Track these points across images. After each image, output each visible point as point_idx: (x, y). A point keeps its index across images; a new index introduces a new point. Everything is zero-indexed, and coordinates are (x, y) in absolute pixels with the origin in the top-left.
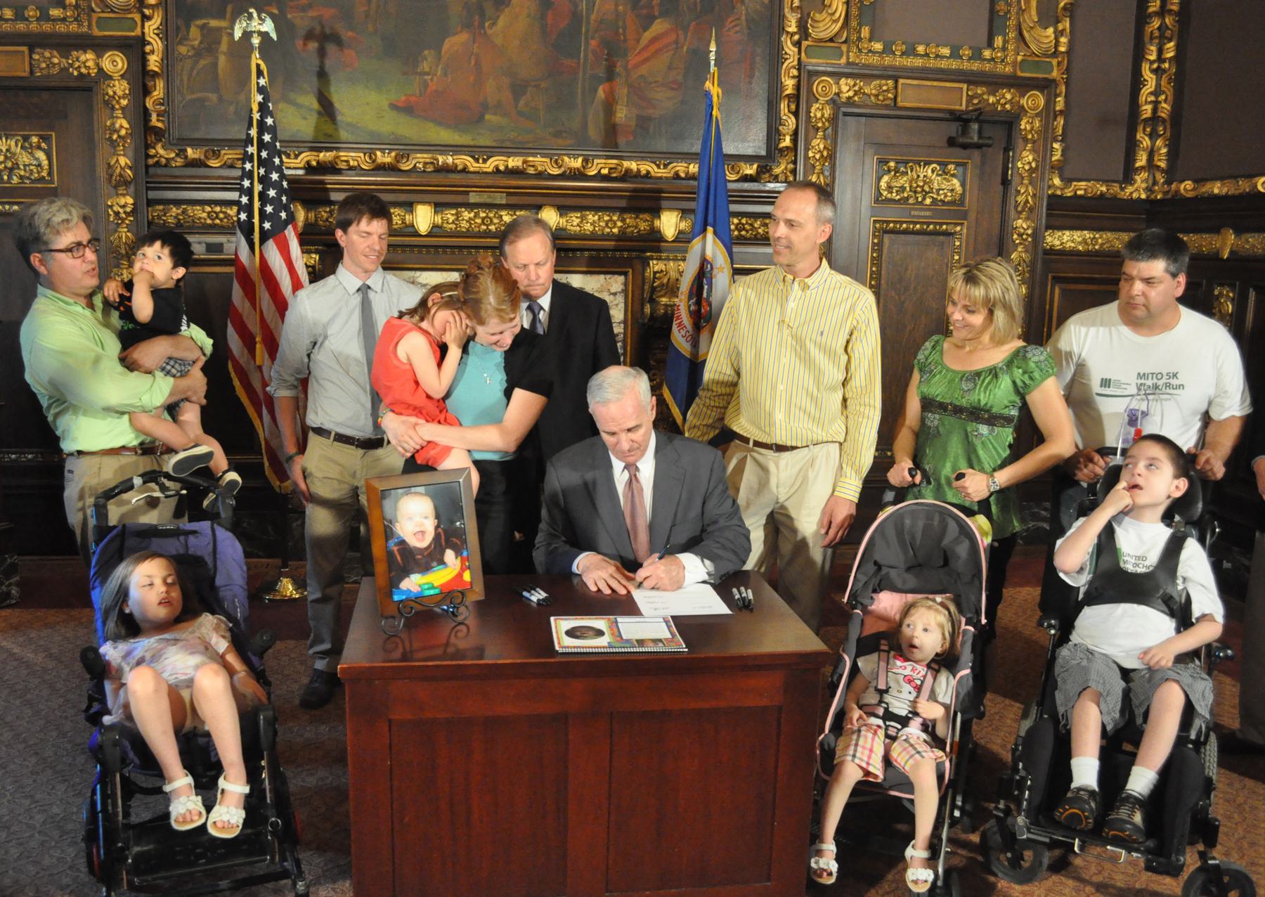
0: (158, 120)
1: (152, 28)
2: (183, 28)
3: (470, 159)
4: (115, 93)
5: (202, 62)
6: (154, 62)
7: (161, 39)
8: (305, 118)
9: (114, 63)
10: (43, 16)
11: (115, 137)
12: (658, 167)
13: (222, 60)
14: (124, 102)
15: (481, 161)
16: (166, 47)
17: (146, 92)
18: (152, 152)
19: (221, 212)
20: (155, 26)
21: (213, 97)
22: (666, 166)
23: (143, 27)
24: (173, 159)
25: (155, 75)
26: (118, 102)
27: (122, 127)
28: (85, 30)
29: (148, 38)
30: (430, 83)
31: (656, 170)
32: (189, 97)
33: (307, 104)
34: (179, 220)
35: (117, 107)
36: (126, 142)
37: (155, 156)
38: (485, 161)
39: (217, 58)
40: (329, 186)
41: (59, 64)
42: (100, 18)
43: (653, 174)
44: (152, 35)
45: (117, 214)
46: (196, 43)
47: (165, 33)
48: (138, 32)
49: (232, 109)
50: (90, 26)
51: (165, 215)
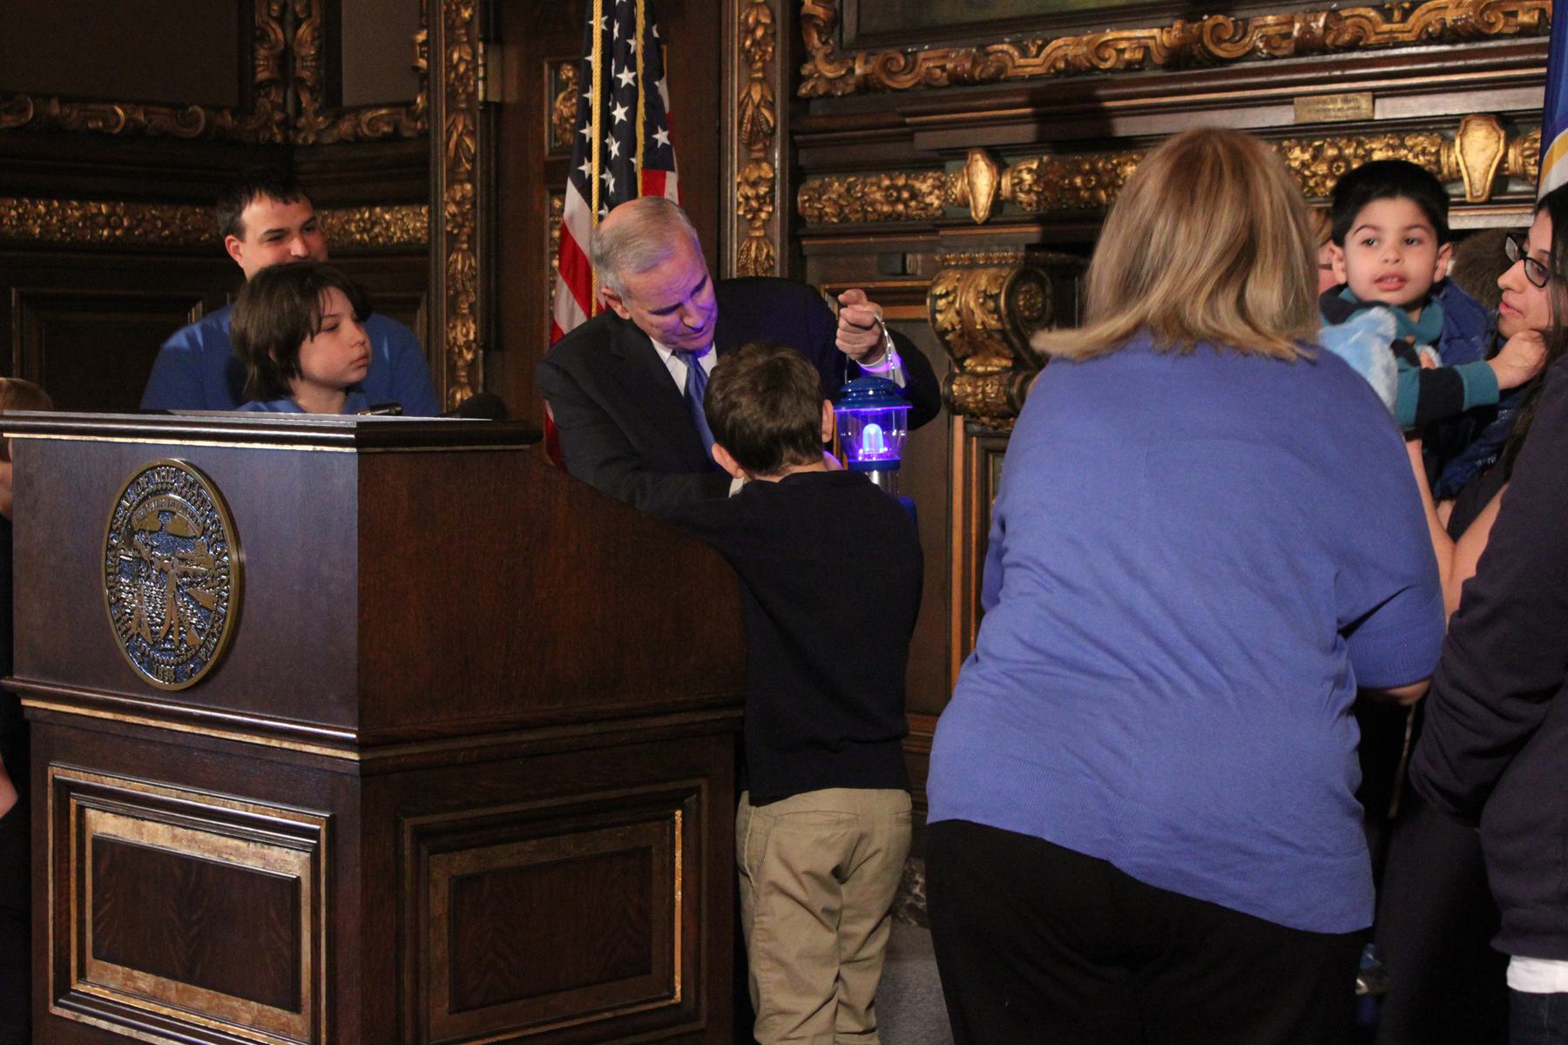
3: (1372, 14)
11: (748, 43)
15: (1397, 15)
18: (806, 70)
19: (905, 186)
24: (842, 77)
27: (758, 22)
34: (841, 207)
36: (765, 52)
37: (810, 76)
38: (1406, 15)
45: (747, 198)
51: (819, 199)
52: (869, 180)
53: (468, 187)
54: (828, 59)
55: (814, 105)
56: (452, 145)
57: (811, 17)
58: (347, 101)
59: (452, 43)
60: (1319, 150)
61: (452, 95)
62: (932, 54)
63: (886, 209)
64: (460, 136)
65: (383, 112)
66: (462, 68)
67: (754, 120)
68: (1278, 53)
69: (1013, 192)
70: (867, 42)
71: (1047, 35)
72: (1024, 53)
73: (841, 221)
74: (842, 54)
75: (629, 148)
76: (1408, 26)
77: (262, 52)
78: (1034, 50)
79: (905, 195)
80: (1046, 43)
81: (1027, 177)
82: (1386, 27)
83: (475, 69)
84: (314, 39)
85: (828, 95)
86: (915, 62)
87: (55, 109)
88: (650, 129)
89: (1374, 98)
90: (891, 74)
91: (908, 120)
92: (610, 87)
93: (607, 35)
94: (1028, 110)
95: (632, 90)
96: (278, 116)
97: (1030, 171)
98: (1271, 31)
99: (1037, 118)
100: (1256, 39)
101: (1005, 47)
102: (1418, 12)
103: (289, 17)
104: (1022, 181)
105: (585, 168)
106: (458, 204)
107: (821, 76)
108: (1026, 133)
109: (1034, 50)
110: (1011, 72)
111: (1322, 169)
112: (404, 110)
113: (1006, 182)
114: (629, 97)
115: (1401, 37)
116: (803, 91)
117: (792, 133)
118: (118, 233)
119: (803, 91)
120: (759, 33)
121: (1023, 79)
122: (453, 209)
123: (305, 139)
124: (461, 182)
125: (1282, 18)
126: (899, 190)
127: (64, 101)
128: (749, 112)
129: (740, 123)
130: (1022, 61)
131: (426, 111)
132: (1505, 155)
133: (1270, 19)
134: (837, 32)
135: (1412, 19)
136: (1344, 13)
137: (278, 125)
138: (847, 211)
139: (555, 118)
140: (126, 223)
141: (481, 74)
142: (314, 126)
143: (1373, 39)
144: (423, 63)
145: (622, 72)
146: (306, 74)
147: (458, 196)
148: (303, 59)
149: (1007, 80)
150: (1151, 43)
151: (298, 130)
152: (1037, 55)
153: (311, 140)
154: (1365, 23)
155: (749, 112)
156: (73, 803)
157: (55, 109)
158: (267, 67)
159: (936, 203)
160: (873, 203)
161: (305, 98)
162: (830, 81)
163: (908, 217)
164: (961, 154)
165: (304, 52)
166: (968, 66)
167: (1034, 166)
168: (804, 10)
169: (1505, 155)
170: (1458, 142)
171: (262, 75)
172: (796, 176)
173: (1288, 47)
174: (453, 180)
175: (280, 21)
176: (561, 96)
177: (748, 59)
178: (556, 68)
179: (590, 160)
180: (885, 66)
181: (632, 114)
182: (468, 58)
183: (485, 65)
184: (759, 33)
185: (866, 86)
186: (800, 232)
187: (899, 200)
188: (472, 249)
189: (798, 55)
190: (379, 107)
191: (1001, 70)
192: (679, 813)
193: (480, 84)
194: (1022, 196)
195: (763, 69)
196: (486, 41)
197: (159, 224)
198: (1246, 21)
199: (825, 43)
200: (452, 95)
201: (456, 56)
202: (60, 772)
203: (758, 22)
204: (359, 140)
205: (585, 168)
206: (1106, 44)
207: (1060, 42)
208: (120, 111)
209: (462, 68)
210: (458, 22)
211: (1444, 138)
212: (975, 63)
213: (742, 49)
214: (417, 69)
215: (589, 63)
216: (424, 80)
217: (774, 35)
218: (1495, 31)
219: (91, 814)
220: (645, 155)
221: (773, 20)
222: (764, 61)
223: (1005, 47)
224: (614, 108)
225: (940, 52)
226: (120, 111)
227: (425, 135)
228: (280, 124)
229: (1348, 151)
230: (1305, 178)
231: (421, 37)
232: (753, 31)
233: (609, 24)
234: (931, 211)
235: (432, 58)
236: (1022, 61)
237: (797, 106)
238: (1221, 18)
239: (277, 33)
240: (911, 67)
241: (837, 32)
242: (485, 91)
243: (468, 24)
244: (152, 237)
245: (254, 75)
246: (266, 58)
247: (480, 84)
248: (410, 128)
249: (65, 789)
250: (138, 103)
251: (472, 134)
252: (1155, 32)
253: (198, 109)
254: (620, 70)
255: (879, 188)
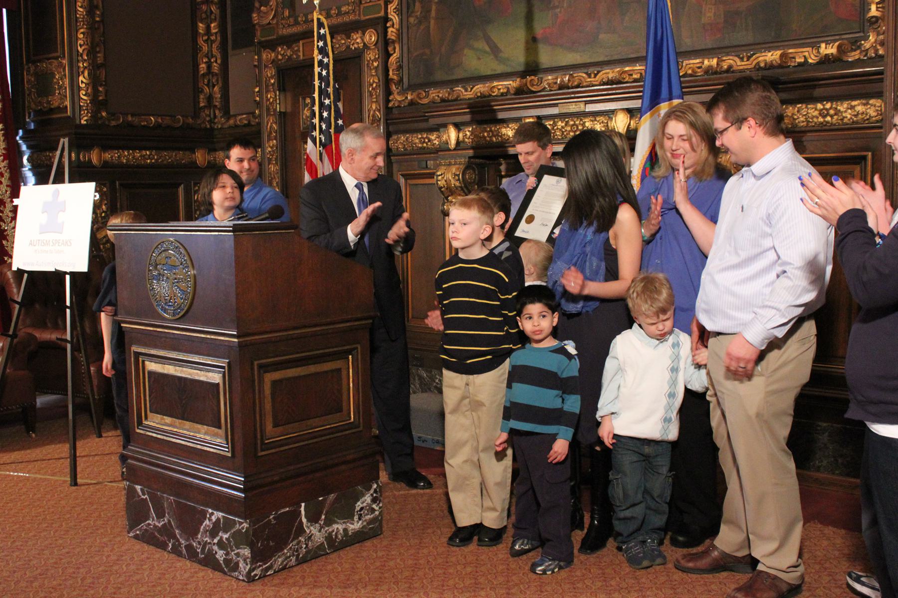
0: (393, 74)
1: (393, 8)
2: (412, 5)
3: (584, 75)
4: (370, 58)
5: (422, 27)
6: (392, 33)
7: (398, 15)
8: (479, 59)
9: (371, 37)
10: (339, 14)
11: (370, 89)
12: (742, 59)
13: (432, 22)
14: (375, 64)
15: (593, 76)
16: (401, 21)
17: (388, 55)
19: (427, 137)
20: (394, 7)
21: (427, 51)
22: (749, 58)
23: (386, 9)
24: (404, 100)
25: (393, 42)
26: (372, 64)
27: (374, 82)
28: (357, 17)
29: (390, 16)
30: (559, 15)
31: (739, 63)
32: (415, 54)
33: (480, 47)
34: (404, 145)
35: (372, 68)
36: (376, 92)
37: (392, 100)
38: (596, 75)
39: (430, 22)
40: (495, 108)
41: (345, 43)
42: (364, 7)
43: (735, 68)
44: (392, 13)
46: (419, 13)
47: (399, 11)
48: (382, 14)
49: (437, 59)
50: (359, 15)
52: (414, 136)
53: (275, 141)
54: (398, 94)
55: (394, 110)
56: (268, 127)
57: (393, 79)
58: (232, 113)
59: (268, 91)
60: (567, 122)
61: (268, 110)
62: (434, 91)
63: (420, 145)
64: (271, 124)
65: (244, 116)
66: (271, 100)
67: (373, 116)
68: (553, 89)
69: (463, 138)
70: (412, 87)
71: (474, 84)
72: (466, 90)
73: (404, 150)
74: (403, 92)
75: (329, 126)
76: (597, 79)
77: (202, 97)
78: (469, 89)
79: (427, 140)
80: (474, 87)
81: (468, 133)
82: (589, 80)
83: (276, 100)
84: (219, 91)
85: (399, 106)
86: (429, 94)
87: (130, 118)
88: (336, 120)
89: (585, 104)
90: (420, 99)
91: (426, 114)
92: (322, 105)
93: (320, 87)
94: (467, 110)
95: (329, 107)
96: (208, 119)
97: (469, 131)
98: (550, 82)
99: (471, 113)
100: (545, 84)
101: (460, 88)
102: (599, 74)
103: (211, 84)
104: (466, 135)
105: (314, 134)
106: (271, 148)
107: (396, 100)
108: (467, 118)
109: (469, 89)
110: (462, 97)
111: (569, 129)
112: (251, 115)
113: (461, 135)
114: (328, 108)
115: (594, 83)
116: (390, 105)
117: (387, 120)
118: (153, 161)
119: (390, 105)
120: (374, 85)
121: (466, 99)
122: (269, 149)
123: (218, 126)
124: (272, 140)
125: (554, 77)
126: (424, 139)
127: (133, 115)
128: (371, 113)
129: (369, 117)
130: (466, 93)
131: (260, 116)
132: (630, 123)
133: (550, 77)
134: (401, 85)
135: (598, 77)
136: (575, 75)
137: (208, 122)
138: (406, 146)
139: (304, 117)
140: (156, 157)
141: (278, 102)
142: (220, 121)
143: (585, 84)
144: (258, 99)
145: (325, 99)
146: (217, 104)
147: (271, 145)
148: (216, 98)
149: (461, 100)
150: (510, 86)
151: (215, 123)
152: (471, 91)
153: (219, 126)
154: (582, 78)
155: (371, 113)
156: (141, 359)
157: (130, 118)
158: (203, 102)
159: (437, 143)
160: (415, 144)
161: (217, 112)
162: (399, 101)
163: (428, 148)
164: (445, 126)
165: (216, 96)
166: (447, 95)
167: (470, 129)
168: (390, 77)
169: (630, 123)
170: (614, 119)
171: (202, 105)
172: (388, 135)
173: (556, 87)
174: (269, 139)
175: (208, 85)
176: (306, 109)
177: (371, 95)
178: (304, 99)
179: (316, 131)
180: (418, 95)
181: (330, 115)
182: (273, 96)
183: (279, 99)
184: (374, 85)
185: (412, 103)
186: (391, 154)
187: (424, 142)
188: (276, 163)
189: (388, 92)
190: (243, 114)
191: (458, 97)
192: (350, 356)
193: (278, 105)
194: (466, 140)
195: (376, 98)
196: (279, 90)
197: (167, 158)
198: (542, 78)
199: (397, 88)
200: (268, 110)
201: (269, 96)
202: (135, 348)
203: (374, 82)
204: (236, 126)
205: (314, 134)
206: (494, 87)
207: (478, 86)
208: (152, 119)
209: (271, 100)
210: (270, 84)
211: (609, 117)
212: (449, 94)
213: (368, 91)
214: (256, 101)
215: (314, 97)
216: (258, 104)
217: (379, 86)
218: (625, 81)
219: (147, 363)
220: (334, 128)
221: (379, 81)
222: (376, 95)
223: (460, 88)
224: (323, 112)
225: (437, 91)
226: (152, 119)
227: (259, 124)
228: (208, 122)
229: (577, 122)
230: (563, 132)
231: (257, 90)
232: (372, 85)
233: (321, 83)
234: (435, 146)
235: (261, 98)
236: (466, 93)
237: (388, 110)
238: (533, 77)
239: (207, 90)
240: (427, 96)
241: (401, 85)
242: (280, 108)
243: (273, 85)
244: (165, 162)
245: (199, 104)
246: (203, 99)
247: (278, 105)
248: (254, 122)
249: (138, 355)
250: (159, 116)
251: (276, 123)
252: (511, 82)
253: (180, 117)
254: (325, 99)
255: (417, 138)
